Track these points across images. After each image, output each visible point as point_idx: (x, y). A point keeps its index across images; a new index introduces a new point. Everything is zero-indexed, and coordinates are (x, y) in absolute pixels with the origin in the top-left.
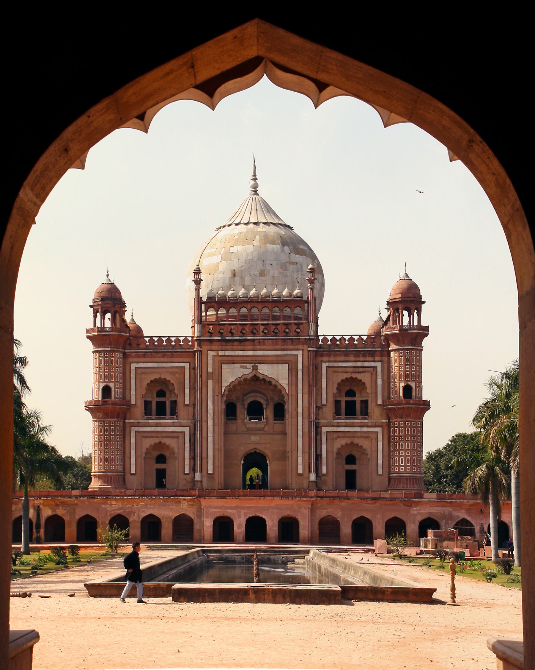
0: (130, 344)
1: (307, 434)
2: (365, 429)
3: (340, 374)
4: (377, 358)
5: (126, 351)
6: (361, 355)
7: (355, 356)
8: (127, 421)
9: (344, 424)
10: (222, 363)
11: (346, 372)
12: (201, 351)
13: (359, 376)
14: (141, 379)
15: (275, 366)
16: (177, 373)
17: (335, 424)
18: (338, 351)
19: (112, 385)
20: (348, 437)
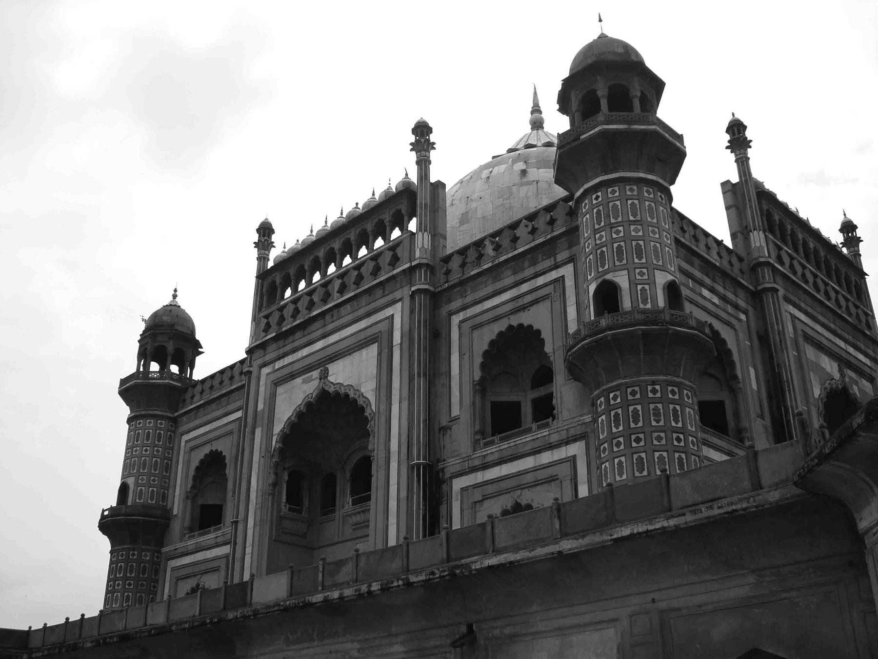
0: (184, 400)
1: (404, 504)
2: (546, 457)
3: (486, 329)
4: (562, 256)
5: (176, 414)
6: (527, 264)
7: (514, 273)
8: (164, 550)
9: (496, 456)
10: (277, 383)
11: (497, 319)
12: (250, 372)
13: (525, 318)
14: (189, 460)
15: (356, 355)
16: (231, 433)
17: (477, 463)
18: (479, 275)
19: (131, 481)
20: (508, 491)
